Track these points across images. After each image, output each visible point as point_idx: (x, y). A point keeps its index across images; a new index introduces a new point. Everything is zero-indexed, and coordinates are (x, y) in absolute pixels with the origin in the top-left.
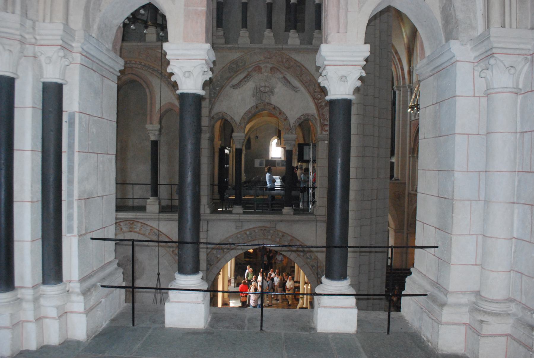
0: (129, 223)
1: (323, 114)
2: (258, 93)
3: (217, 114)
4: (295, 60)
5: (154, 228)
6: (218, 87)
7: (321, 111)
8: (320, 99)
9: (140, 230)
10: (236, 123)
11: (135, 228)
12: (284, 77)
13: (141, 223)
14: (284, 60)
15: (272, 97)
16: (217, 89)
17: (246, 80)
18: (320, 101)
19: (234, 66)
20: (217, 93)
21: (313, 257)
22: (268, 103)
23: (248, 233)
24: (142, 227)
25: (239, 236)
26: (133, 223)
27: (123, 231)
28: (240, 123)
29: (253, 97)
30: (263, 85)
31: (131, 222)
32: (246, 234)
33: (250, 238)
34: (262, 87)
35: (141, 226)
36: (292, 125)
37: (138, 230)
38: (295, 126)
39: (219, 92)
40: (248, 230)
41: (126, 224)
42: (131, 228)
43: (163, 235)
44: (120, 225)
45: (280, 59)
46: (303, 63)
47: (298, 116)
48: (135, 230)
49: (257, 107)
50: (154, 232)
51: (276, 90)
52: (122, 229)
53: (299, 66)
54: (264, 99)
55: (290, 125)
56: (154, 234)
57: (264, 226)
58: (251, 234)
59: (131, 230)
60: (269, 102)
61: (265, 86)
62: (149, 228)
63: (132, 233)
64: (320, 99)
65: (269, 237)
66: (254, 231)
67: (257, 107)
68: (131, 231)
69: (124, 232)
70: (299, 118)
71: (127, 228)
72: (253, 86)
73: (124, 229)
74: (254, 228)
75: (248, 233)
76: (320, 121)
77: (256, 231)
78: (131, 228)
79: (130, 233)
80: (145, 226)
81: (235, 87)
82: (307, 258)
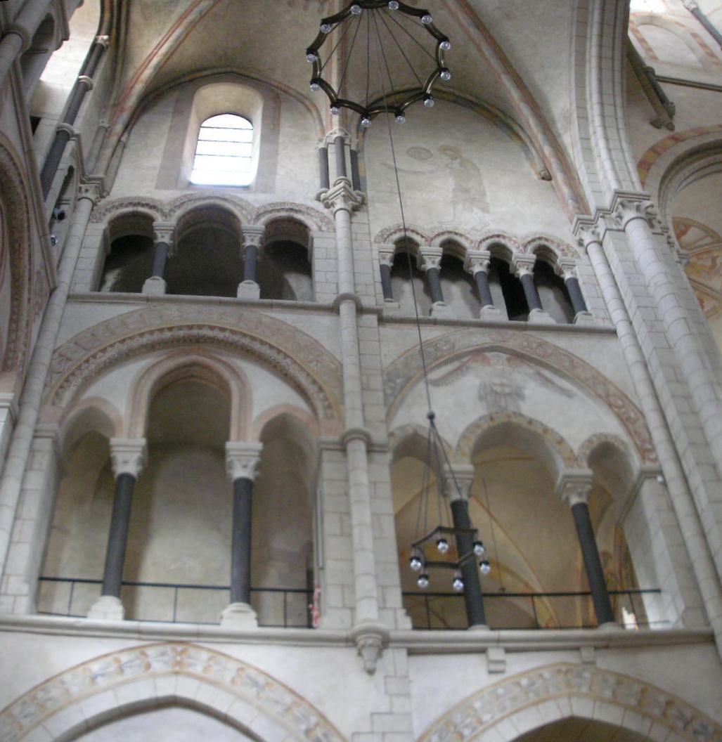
0: (174, 650)
1: (636, 432)
2: (488, 393)
3: (401, 428)
4: (554, 346)
5: (250, 666)
6: (399, 378)
7: (631, 427)
8: (623, 406)
9: (206, 669)
10: (450, 446)
11: (191, 665)
12: (539, 374)
13: (210, 650)
14: (534, 345)
15: (520, 402)
16: (398, 381)
17: (459, 372)
18: (623, 410)
19: (432, 350)
20: (398, 387)
21: (711, 729)
22: (515, 413)
23: (524, 682)
24: (212, 663)
25: (500, 691)
26: (183, 652)
27: (152, 670)
28: (458, 446)
29: (481, 399)
30: (497, 381)
31: (180, 648)
32: (518, 684)
33: (531, 695)
34: (495, 384)
35: (210, 659)
36: (576, 451)
37: (198, 669)
38: (584, 454)
39: (402, 388)
40: (524, 674)
41: (163, 654)
42: (179, 663)
43: (276, 685)
44: (144, 654)
45: (525, 344)
46: (571, 350)
47: (585, 436)
48: (191, 670)
49: (492, 419)
50: (249, 677)
51: (527, 392)
52: (148, 666)
53: (567, 356)
54: (503, 404)
55: (572, 451)
56: (248, 680)
57: (564, 663)
58: (532, 684)
59: (177, 669)
60: (515, 410)
61: (502, 385)
62: (233, 666)
63: (180, 678)
64: (623, 406)
65: (585, 689)
66: (541, 676)
67: (492, 419)
68: (176, 673)
69: (155, 676)
70: (589, 441)
71: (165, 662)
72: (477, 382)
73: (158, 666)
74: (539, 668)
75: (524, 682)
76: (636, 444)
77: (547, 674)
78: (179, 663)
79: (173, 679)
80: (222, 659)
81: (437, 383)
82: (696, 732)
